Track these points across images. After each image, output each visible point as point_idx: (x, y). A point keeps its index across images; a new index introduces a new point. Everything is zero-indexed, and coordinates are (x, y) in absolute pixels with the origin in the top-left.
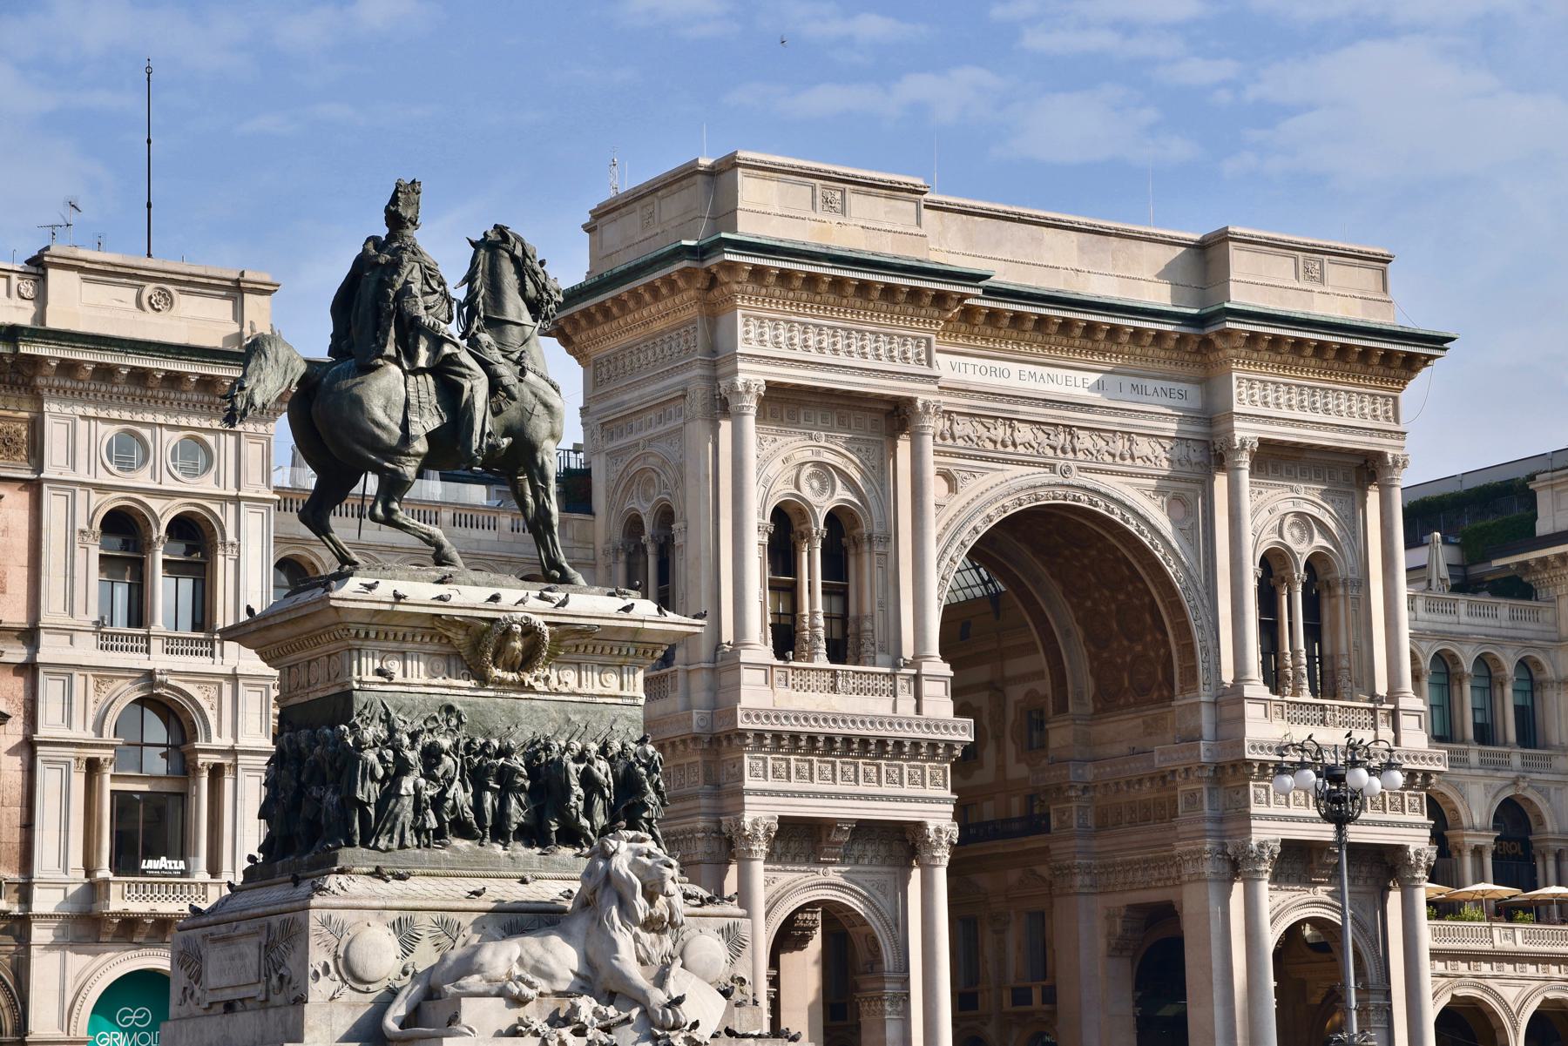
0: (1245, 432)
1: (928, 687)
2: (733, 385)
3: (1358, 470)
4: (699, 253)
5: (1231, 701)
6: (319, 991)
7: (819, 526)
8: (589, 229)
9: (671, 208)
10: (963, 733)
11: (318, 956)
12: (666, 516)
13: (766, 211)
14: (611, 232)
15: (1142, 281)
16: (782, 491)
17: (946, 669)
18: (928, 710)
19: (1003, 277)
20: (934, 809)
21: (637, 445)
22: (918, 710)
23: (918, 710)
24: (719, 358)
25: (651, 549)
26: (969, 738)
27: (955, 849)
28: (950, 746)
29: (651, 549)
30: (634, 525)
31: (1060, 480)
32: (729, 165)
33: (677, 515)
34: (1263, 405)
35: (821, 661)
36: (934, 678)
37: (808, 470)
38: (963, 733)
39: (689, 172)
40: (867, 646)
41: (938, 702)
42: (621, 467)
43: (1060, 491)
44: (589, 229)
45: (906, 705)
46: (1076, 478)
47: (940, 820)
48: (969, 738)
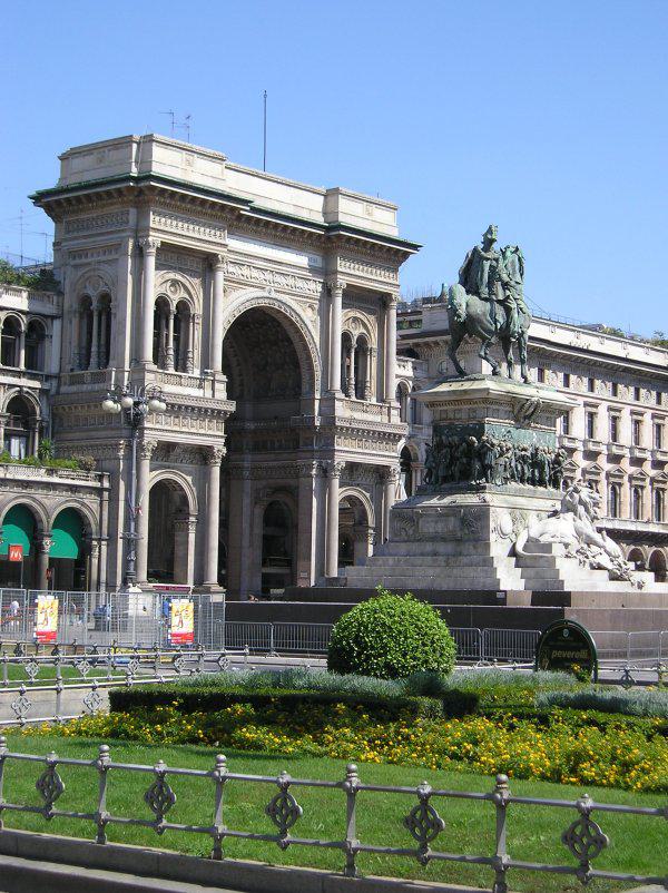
0: (342, 281)
1: (217, 385)
2: (147, 241)
3: (377, 303)
4: (136, 180)
5: (329, 399)
6: (493, 537)
7: (173, 308)
8: (64, 158)
9: (114, 155)
10: (232, 407)
11: (492, 525)
12: (106, 299)
13: (166, 163)
14: (77, 163)
15: (310, 208)
16: (162, 290)
17: (224, 378)
18: (217, 396)
19: (258, 203)
20: (213, 436)
21: (89, 264)
22: (213, 396)
23: (213, 396)
24: (141, 231)
25: (95, 314)
26: (233, 409)
27: (223, 459)
28: (225, 412)
29: (95, 314)
30: (85, 301)
31: (268, 295)
32: (149, 140)
33: (113, 298)
34: (350, 272)
35: (171, 370)
36: (219, 381)
37: (169, 283)
38: (232, 407)
39: (128, 140)
40: (189, 365)
41: (221, 392)
42: (80, 273)
43: (266, 301)
44: (64, 158)
45: (208, 394)
46: (274, 295)
47: (219, 446)
48: (233, 409)
